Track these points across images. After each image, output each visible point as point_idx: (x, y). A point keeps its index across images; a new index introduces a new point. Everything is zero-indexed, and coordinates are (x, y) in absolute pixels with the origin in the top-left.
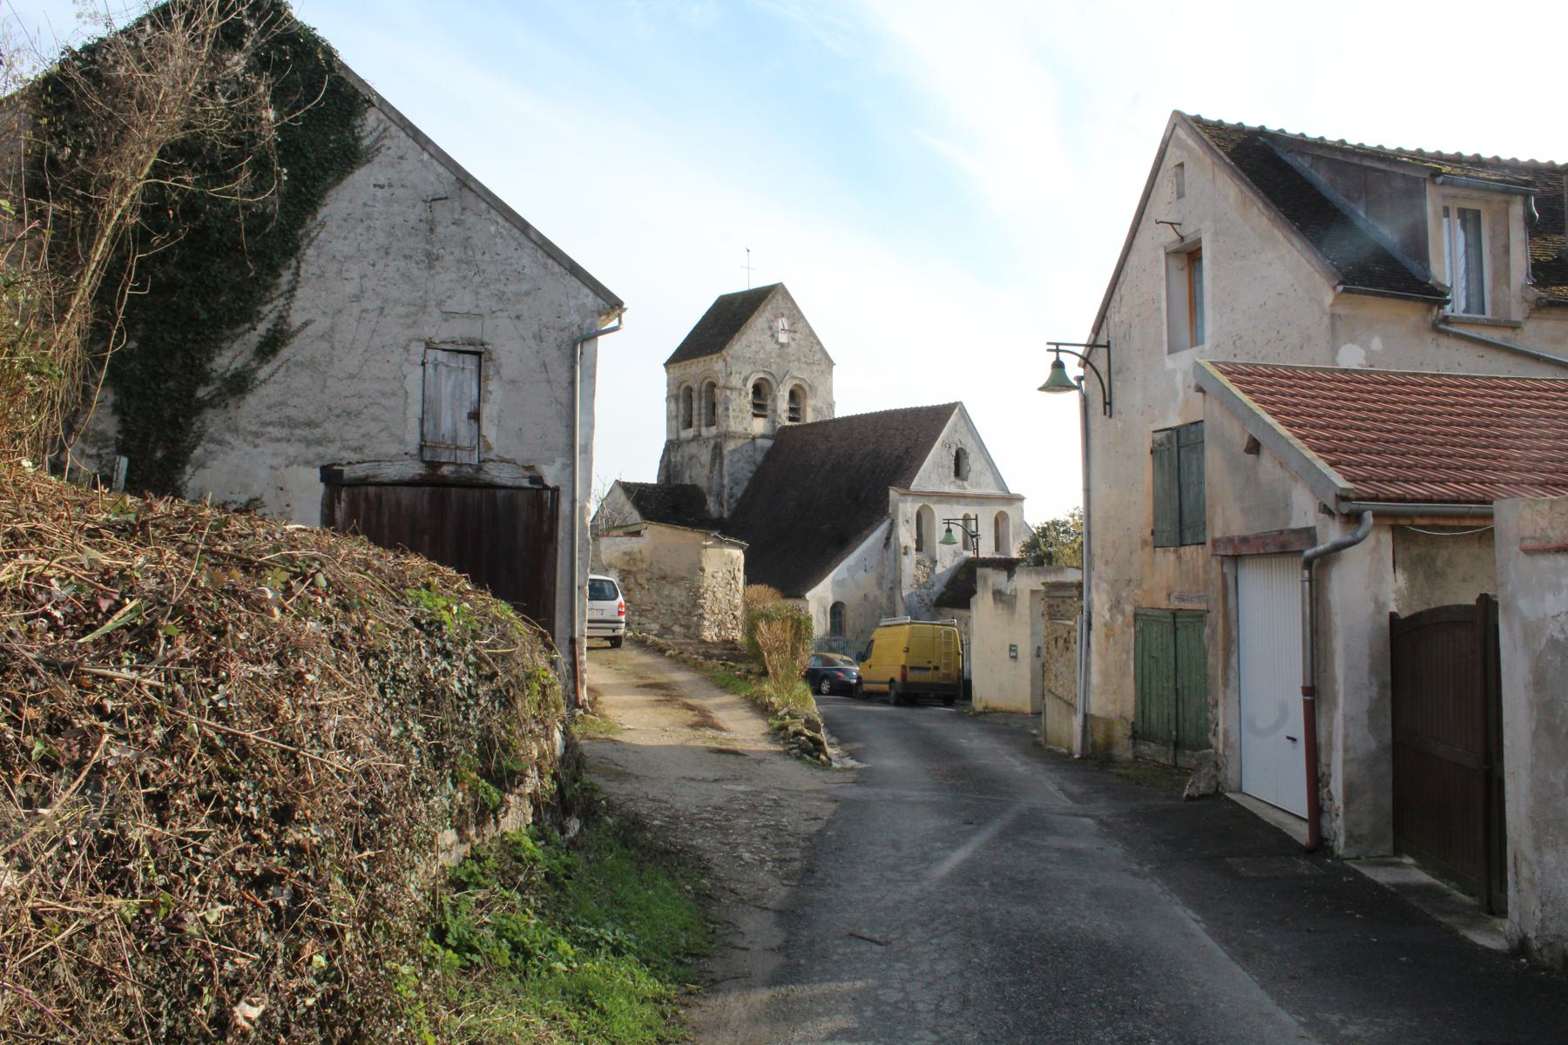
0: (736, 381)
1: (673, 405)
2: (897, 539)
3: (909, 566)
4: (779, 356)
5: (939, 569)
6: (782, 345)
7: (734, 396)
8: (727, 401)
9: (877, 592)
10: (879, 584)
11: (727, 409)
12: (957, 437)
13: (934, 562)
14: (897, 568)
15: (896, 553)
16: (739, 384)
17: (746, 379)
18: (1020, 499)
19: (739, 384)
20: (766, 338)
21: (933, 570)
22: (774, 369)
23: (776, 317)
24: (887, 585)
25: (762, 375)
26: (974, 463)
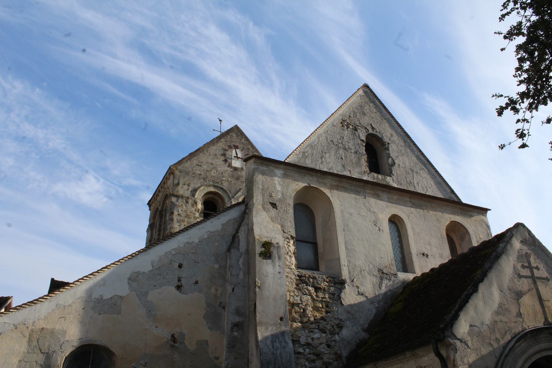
0: (182, 190)
1: (150, 232)
2: (250, 231)
3: (278, 279)
4: (232, 176)
5: (350, 297)
6: (236, 169)
7: (180, 202)
8: (173, 205)
9: (205, 333)
10: (214, 316)
11: (172, 213)
12: (365, 121)
13: (339, 283)
14: (249, 285)
15: (249, 254)
16: (188, 194)
17: (195, 191)
18: (483, 211)
19: (188, 194)
20: (219, 161)
21: (337, 297)
22: (225, 185)
23: (230, 147)
24: (229, 318)
25: (212, 189)
26: (395, 149)
